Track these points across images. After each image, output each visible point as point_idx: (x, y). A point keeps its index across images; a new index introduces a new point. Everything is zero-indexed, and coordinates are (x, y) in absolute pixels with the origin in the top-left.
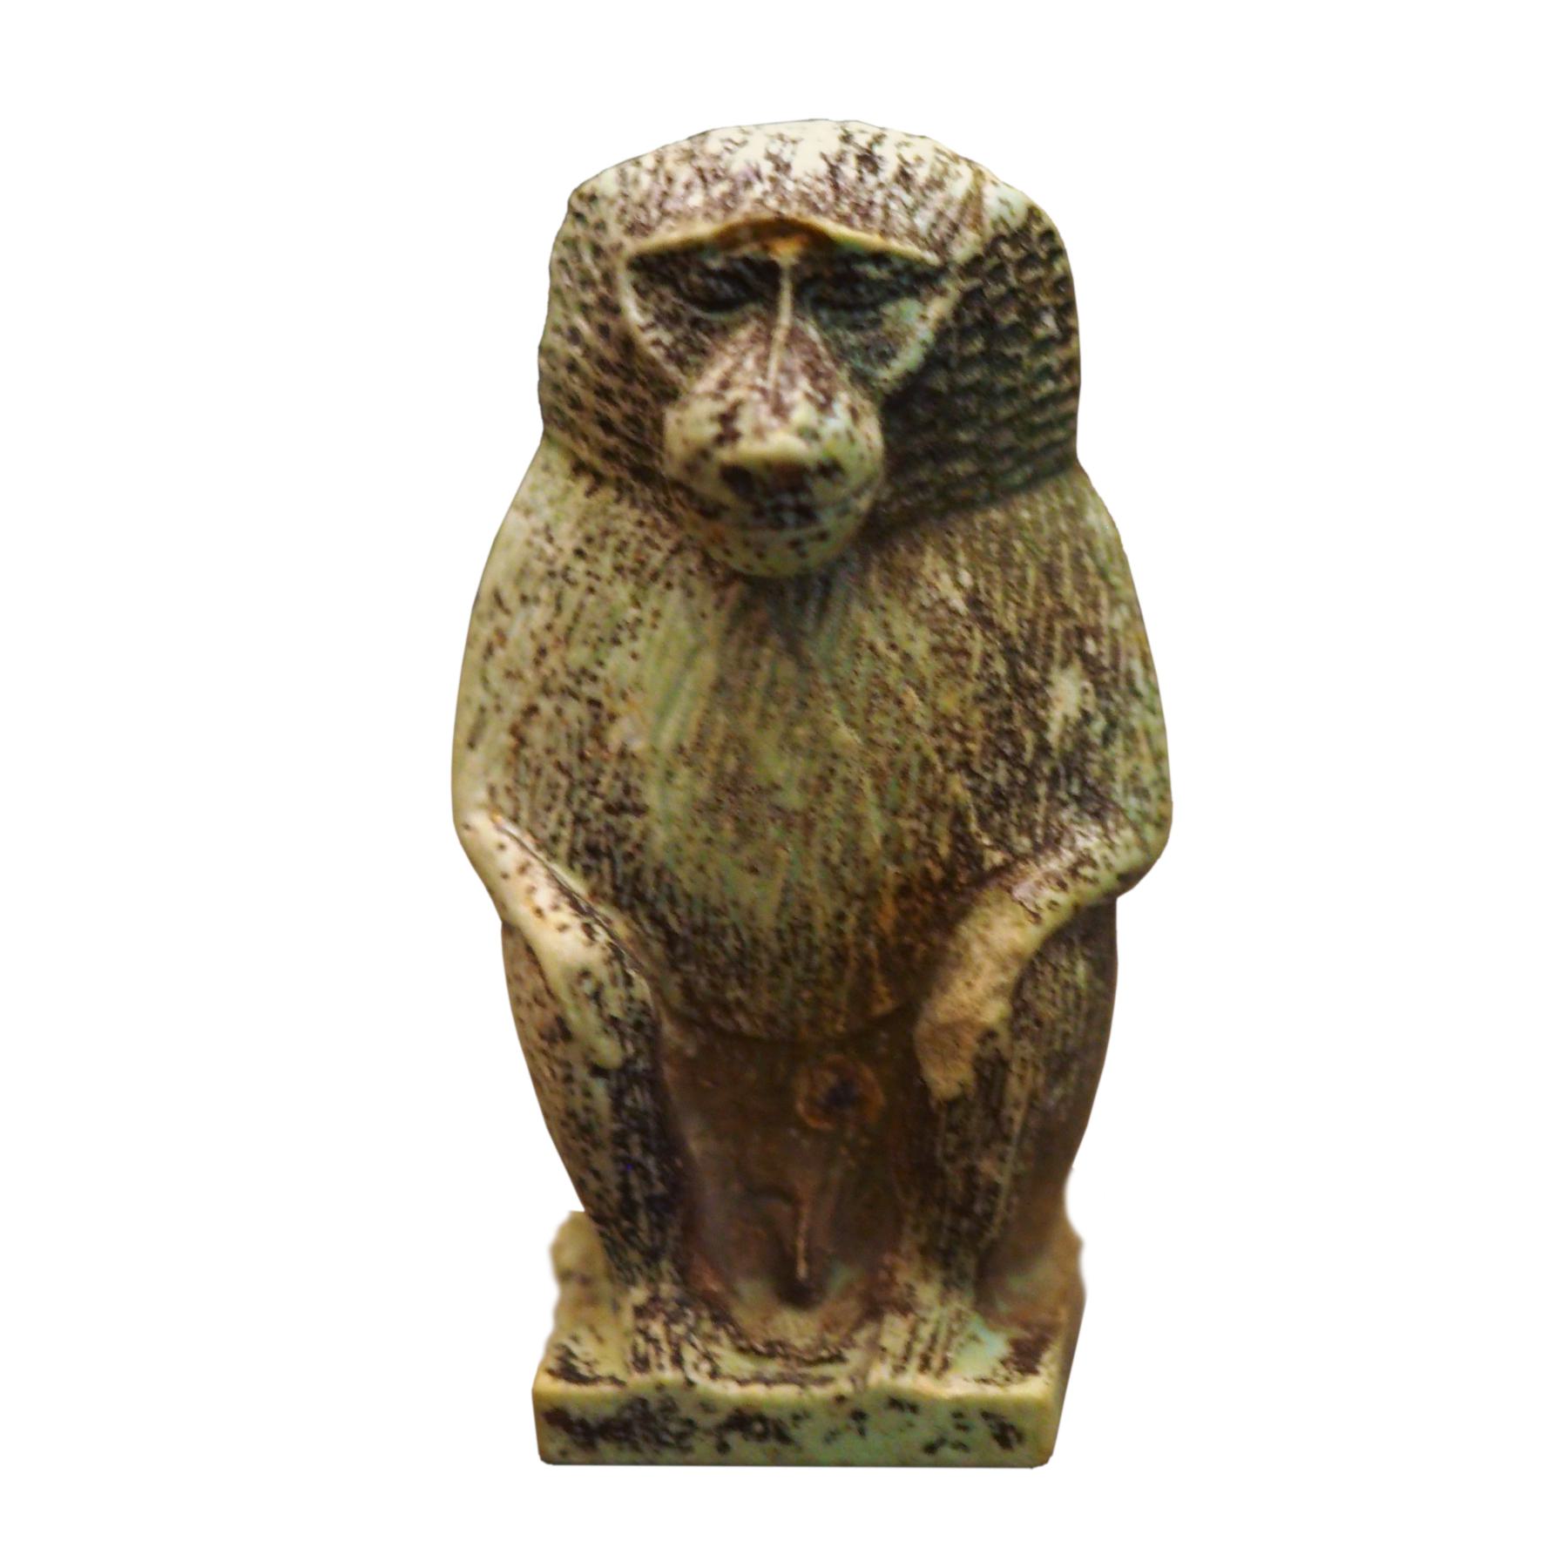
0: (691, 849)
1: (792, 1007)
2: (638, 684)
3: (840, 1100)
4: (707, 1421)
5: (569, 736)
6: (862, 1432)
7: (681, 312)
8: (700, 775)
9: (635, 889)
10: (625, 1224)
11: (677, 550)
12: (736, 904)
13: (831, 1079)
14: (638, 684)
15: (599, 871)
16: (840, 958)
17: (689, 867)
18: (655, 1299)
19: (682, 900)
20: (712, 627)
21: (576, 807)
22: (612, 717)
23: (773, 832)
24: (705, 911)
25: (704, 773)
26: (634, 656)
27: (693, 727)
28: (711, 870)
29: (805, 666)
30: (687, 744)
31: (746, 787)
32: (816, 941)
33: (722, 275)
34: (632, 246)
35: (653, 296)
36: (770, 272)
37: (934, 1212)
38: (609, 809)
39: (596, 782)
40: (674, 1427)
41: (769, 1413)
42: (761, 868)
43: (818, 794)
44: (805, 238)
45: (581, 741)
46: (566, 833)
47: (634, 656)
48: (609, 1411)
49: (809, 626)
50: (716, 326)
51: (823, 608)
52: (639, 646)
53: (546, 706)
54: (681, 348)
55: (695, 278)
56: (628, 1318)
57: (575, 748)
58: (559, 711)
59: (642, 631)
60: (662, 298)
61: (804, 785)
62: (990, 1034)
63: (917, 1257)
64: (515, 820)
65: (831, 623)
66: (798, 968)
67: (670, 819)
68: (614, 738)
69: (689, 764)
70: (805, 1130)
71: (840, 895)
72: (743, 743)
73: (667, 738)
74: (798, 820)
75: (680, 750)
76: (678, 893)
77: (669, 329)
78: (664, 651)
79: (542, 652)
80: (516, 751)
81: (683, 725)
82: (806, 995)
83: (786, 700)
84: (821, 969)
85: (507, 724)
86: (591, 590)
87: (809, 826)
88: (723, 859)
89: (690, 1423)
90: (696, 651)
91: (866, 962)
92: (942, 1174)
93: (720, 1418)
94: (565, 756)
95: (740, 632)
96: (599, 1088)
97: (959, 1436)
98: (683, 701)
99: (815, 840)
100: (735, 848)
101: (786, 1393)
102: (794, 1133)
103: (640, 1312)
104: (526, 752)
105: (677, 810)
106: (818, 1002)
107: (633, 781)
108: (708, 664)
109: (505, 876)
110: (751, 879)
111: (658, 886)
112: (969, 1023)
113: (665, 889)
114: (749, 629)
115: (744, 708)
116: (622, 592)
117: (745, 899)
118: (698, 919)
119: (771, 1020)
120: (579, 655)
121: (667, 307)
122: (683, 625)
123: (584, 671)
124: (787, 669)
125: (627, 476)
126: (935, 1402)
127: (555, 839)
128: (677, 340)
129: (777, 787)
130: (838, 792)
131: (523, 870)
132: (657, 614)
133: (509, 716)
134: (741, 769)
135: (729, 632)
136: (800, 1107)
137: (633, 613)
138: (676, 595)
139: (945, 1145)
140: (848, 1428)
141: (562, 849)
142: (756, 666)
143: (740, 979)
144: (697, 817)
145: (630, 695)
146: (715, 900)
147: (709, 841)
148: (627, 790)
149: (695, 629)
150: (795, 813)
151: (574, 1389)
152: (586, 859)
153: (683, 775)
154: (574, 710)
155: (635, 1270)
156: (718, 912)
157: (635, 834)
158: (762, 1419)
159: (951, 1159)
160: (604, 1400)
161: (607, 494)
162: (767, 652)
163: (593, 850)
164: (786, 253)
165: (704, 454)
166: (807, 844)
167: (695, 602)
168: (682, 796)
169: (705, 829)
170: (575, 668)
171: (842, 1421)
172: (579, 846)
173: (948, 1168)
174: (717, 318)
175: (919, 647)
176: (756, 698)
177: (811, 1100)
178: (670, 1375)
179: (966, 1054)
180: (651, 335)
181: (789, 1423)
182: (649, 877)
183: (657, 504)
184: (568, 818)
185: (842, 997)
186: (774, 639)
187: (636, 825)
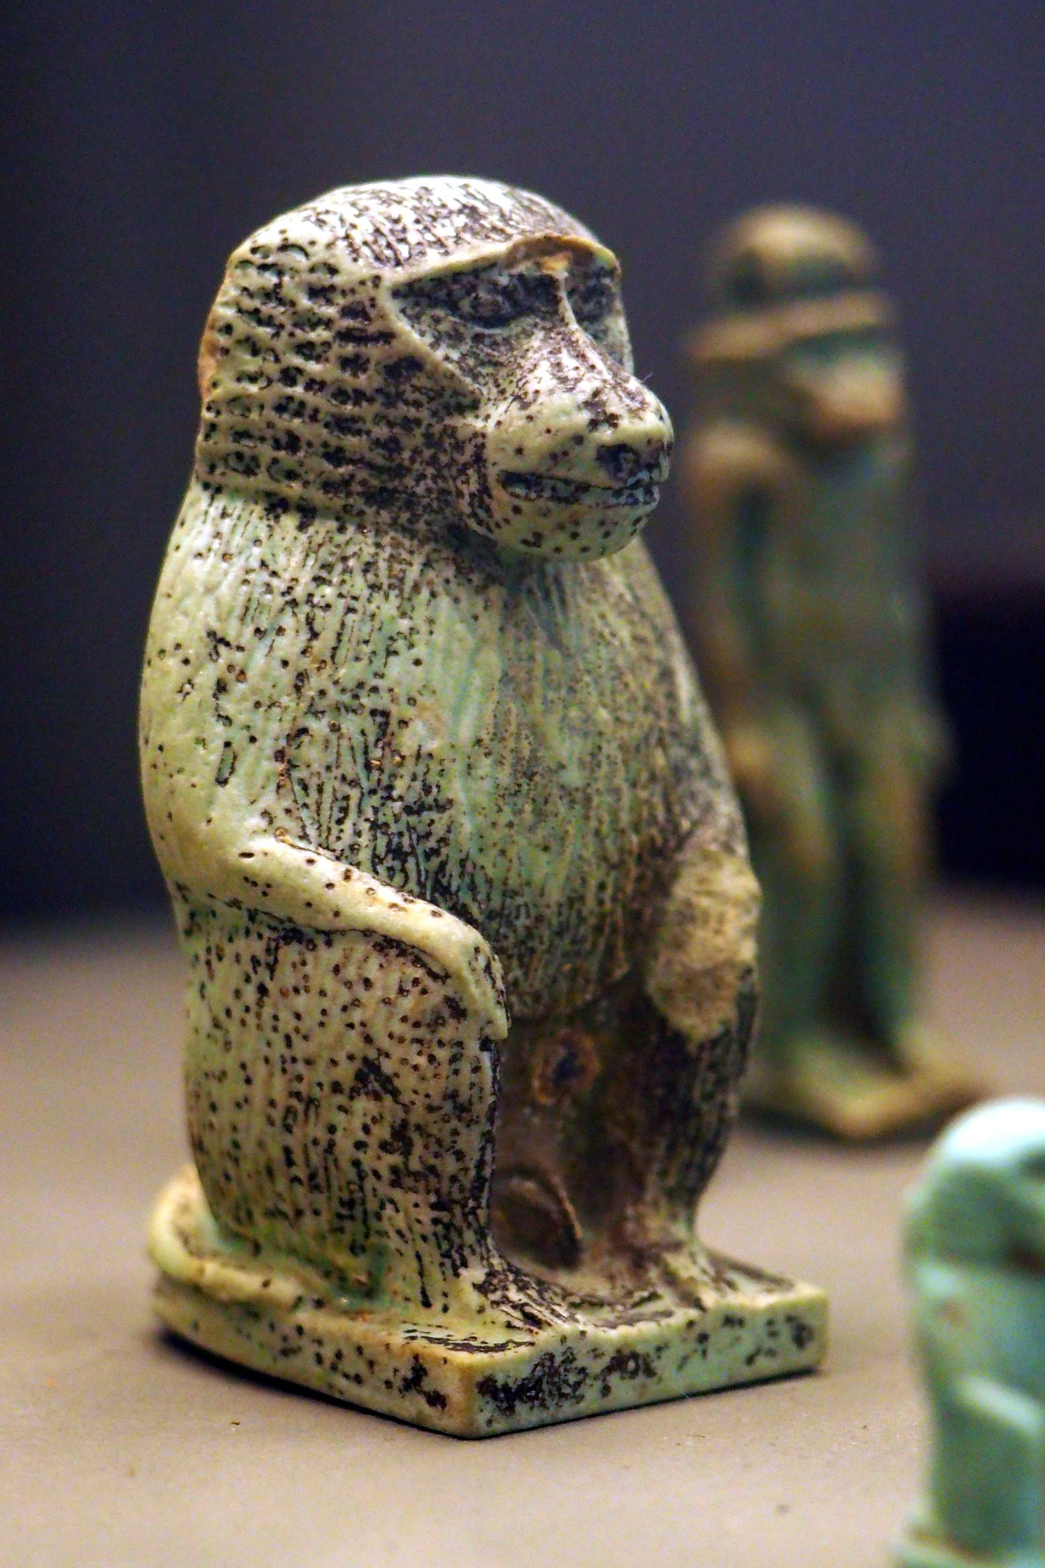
0: (496, 835)
1: (554, 980)
2: (426, 687)
3: (565, 1071)
4: (596, 1367)
5: (352, 748)
6: (704, 1353)
7: (462, 329)
8: (501, 763)
9: (437, 881)
10: (471, 1203)
11: (427, 564)
12: (528, 884)
13: (562, 1052)
14: (426, 687)
15: (403, 870)
16: (598, 929)
17: (494, 852)
18: (491, 1274)
19: (483, 889)
20: (489, 623)
21: (370, 814)
22: (404, 723)
23: (562, 808)
24: (504, 894)
25: (504, 761)
26: (417, 662)
27: (489, 718)
28: (512, 853)
29: (567, 655)
30: (485, 737)
31: (540, 769)
32: (585, 913)
33: (505, 292)
34: (393, 275)
35: (426, 319)
36: (548, 285)
37: (686, 1153)
38: (408, 810)
39: (390, 788)
40: (572, 1378)
41: (640, 1349)
42: (554, 845)
43: (592, 771)
44: (569, 254)
45: (366, 752)
46: (364, 840)
47: (417, 662)
48: (525, 1372)
49: (560, 619)
50: (499, 339)
51: (563, 602)
52: (420, 651)
53: (319, 727)
54: (471, 362)
55: (483, 295)
56: (474, 1299)
57: (361, 760)
58: (335, 728)
59: (419, 639)
60: (437, 320)
61: (581, 763)
62: (748, 971)
63: (664, 1203)
64: (304, 837)
65: (572, 615)
66: (567, 940)
67: (475, 809)
68: (408, 741)
69: (487, 754)
70: (536, 1107)
71: (604, 866)
72: (533, 727)
73: (466, 732)
74: (579, 796)
75: (479, 742)
76: (479, 880)
77: (453, 347)
78: (448, 654)
79: (302, 676)
80: (287, 773)
81: (479, 718)
82: (567, 967)
83: (559, 686)
84: (584, 939)
85: (269, 752)
86: (351, 610)
87: (588, 799)
88: (522, 841)
89: (582, 1370)
90: (477, 650)
91: (614, 931)
92: (698, 1114)
93: (605, 1361)
94: (349, 768)
95: (512, 631)
96: (486, 1059)
97: (769, 1343)
98: (476, 696)
99: (592, 813)
100: (532, 829)
101: (646, 1329)
102: (527, 1111)
103: (482, 1288)
104: (296, 774)
105: (483, 800)
106: (575, 973)
107: (433, 778)
108: (493, 660)
109: (330, 886)
110: (544, 857)
111: (462, 875)
112: (730, 963)
113: (467, 880)
114: (517, 625)
115: (528, 697)
116: (388, 607)
117: (538, 877)
118: (496, 903)
119: (537, 997)
120: (348, 673)
121: (443, 327)
122: (460, 628)
123: (361, 685)
124: (556, 656)
125: (358, 503)
126: (755, 1313)
127: (353, 848)
128: (464, 356)
129: (562, 767)
130: (605, 768)
131: (347, 877)
132: (431, 621)
133: (268, 745)
134: (533, 751)
135: (502, 629)
136: (536, 1083)
137: (404, 624)
138: (444, 602)
139: (704, 1082)
140: (696, 1351)
141: (364, 855)
142: (532, 658)
143: (520, 957)
144: (501, 802)
145: (418, 698)
146: (514, 882)
147: (510, 825)
148: (427, 789)
149: (473, 631)
150: (577, 790)
151: (498, 1356)
152: (389, 862)
153: (485, 766)
154: (350, 725)
155: (467, 1252)
156: (515, 893)
157: (439, 830)
158: (634, 1356)
159: (708, 1097)
160: (522, 1361)
161: (322, 528)
162: (537, 643)
163: (397, 852)
164: (558, 268)
165: (579, 439)
166: (586, 818)
167: (464, 604)
168: (488, 785)
169: (507, 816)
170: (351, 685)
171: (692, 1345)
172: (381, 850)
173: (705, 1107)
174: (498, 332)
175: (625, 633)
176: (538, 685)
177: (542, 1076)
178: (567, 1327)
179: (727, 993)
180: (439, 354)
181: (653, 1354)
182: (453, 868)
183: (394, 524)
184: (365, 826)
185: (593, 966)
186: (540, 632)
187: (441, 821)
